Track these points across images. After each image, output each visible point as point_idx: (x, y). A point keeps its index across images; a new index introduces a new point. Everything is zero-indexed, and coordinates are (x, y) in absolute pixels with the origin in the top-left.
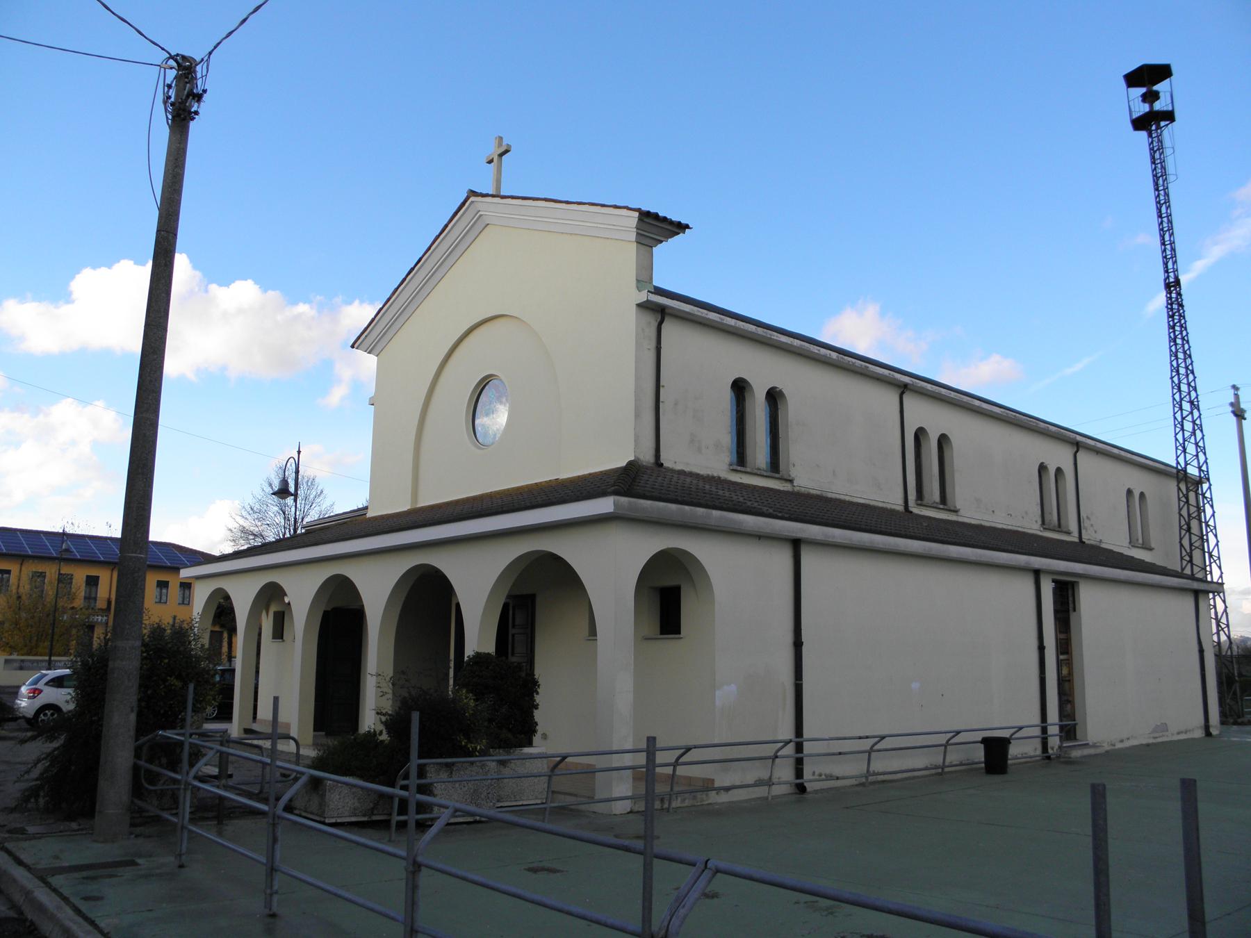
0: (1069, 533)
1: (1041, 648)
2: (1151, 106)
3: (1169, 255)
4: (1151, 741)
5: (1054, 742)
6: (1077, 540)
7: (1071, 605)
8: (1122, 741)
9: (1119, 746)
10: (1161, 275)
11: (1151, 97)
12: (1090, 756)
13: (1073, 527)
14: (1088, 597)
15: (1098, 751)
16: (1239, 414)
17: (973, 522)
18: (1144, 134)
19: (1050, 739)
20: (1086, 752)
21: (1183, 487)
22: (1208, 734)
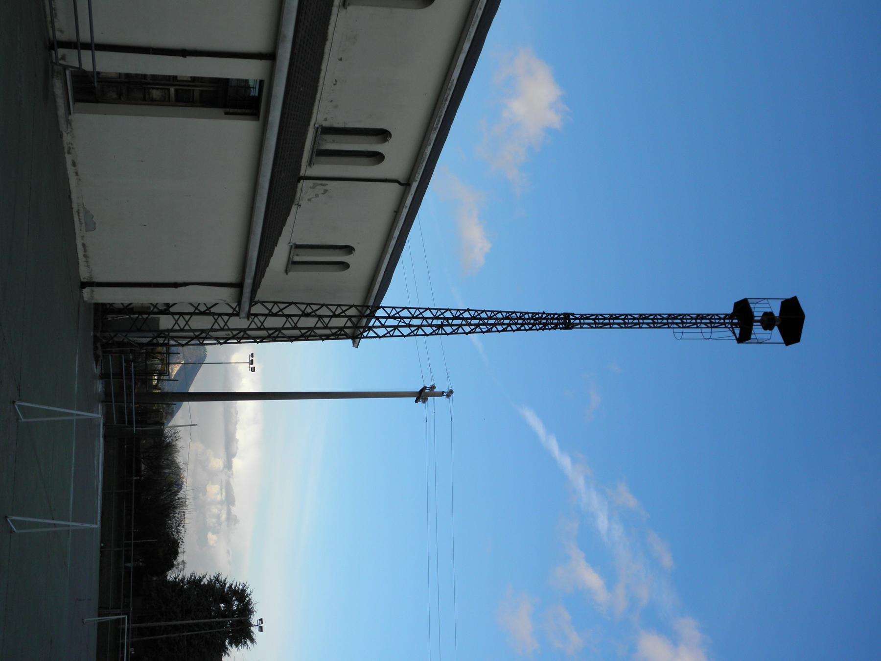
0: (310, 163)
1: (184, 53)
2: (757, 321)
3: (598, 321)
4: (75, 206)
5: (71, 58)
6: (302, 173)
7: (231, 110)
8: (74, 164)
9: (69, 159)
10: (578, 310)
11: (768, 321)
12: (56, 108)
13: (319, 170)
14: (239, 131)
15: (62, 121)
16: (422, 395)
17: (331, 28)
18: (730, 310)
19: (75, 52)
20: (61, 111)
21: (352, 312)
22: (84, 285)
